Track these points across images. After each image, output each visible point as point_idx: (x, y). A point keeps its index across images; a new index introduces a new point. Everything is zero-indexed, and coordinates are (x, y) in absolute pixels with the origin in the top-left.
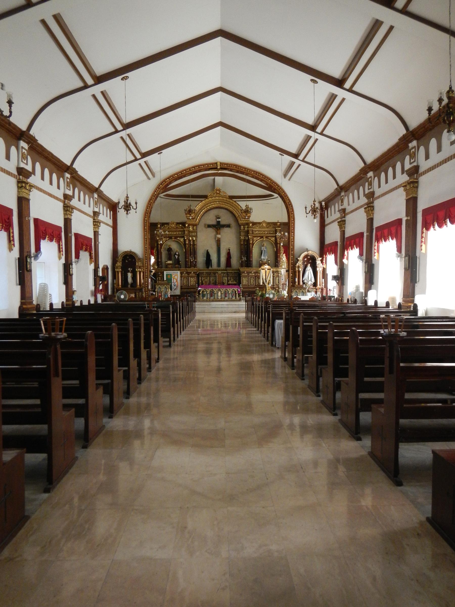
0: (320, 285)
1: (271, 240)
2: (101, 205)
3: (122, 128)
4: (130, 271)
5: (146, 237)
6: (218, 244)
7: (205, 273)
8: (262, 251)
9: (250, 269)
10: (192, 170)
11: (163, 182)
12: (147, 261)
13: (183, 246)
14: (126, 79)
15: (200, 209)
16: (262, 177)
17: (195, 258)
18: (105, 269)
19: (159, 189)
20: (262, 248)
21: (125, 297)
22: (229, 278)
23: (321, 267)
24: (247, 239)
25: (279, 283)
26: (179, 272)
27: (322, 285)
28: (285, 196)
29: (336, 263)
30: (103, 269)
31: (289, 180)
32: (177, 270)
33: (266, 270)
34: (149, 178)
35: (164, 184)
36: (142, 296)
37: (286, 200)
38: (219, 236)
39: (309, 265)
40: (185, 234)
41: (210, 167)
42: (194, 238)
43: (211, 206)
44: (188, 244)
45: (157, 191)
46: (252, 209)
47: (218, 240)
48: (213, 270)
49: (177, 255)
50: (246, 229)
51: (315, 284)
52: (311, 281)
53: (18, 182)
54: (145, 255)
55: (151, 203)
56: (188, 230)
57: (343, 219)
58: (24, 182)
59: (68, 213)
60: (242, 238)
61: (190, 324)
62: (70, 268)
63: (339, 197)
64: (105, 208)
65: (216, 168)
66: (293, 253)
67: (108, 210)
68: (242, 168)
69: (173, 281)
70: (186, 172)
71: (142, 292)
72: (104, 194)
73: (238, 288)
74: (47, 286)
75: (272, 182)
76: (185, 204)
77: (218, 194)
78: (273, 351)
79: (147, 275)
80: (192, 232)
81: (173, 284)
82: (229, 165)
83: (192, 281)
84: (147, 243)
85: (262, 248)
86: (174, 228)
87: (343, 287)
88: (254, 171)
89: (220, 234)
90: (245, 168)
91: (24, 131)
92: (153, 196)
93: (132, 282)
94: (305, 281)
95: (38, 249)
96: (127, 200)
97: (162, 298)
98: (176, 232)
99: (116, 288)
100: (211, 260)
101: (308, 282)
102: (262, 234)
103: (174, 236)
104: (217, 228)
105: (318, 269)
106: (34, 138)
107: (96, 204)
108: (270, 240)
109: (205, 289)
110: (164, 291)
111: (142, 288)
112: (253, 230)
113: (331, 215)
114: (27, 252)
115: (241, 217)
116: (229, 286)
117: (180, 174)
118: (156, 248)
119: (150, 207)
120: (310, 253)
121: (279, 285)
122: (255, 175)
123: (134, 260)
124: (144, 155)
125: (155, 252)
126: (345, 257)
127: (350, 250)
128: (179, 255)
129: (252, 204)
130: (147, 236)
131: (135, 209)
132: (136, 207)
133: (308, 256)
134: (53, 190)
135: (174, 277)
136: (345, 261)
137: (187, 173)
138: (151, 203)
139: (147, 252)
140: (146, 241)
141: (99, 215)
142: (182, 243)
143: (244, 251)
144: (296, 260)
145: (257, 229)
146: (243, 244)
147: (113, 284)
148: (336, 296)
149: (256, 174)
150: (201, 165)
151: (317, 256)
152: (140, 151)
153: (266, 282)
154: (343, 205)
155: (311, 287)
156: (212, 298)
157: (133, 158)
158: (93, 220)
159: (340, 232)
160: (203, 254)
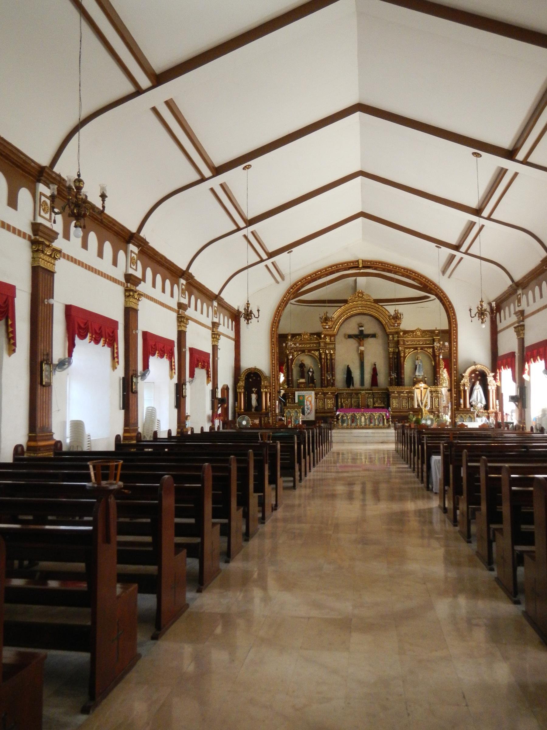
0: (493, 408)
1: (428, 352)
2: (222, 315)
3: (244, 225)
4: (255, 392)
5: (273, 351)
8: (416, 366)
9: (402, 388)
10: (329, 270)
11: (293, 286)
12: (275, 380)
13: (318, 361)
14: (248, 168)
15: (339, 316)
16: (415, 275)
17: (333, 375)
18: (225, 389)
19: (289, 293)
20: (417, 362)
21: (248, 423)
22: (375, 399)
23: (494, 385)
24: (397, 351)
25: (438, 405)
26: (313, 392)
27: (496, 408)
28: (444, 298)
29: (514, 379)
30: (223, 390)
31: (449, 277)
32: (311, 390)
33: (422, 389)
34: (277, 282)
35: (295, 288)
36: (269, 421)
37: (446, 303)
38: (362, 348)
39: (478, 382)
40: (320, 347)
41: (351, 266)
42: (332, 351)
43: (352, 313)
44: (324, 359)
45: (286, 296)
46: (402, 315)
47: (360, 353)
48: (356, 390)
49: (310, 371)
50: (396, 339)
51: (486, 407)
52: (481, 403)
53: (126, 290)
54: (273, 372)
55: (280, 310)
56: (325, 342)
57: (522, 323)
58: (132, 290)
59: (182, 324)
60: (391, 350)
61: (324, 458)
62: (183, 389)
63: (514, 297)
64: (226, 317)
65: (357, 267)
66: (456, 367)
67: (230, 320)
68: (389, 266)
69: (305, 404)
70: (321, 273)
71: (268, 417)
72: (225, 302)
73: (386, 412)
74: (155, 410)
75: (427, 281)
76: (321, 311)
77: (361, 297)
78: (429, 498)
79: (275, 397)
80: (329, 344)
81: (306, 407)
82: (374, 262)
83: (330, 403)
84: (274, 358)
85: (417, 362)
86: (307, 339)
87: (525, 411)
88: (404, 269)
89: (363, 346)
90: (393, 266)
91: (134, 234)
92: (282, 302)
93: (257, 405)
94: (473, 403)
95: (146, 366)
96: (248, 307)
97: (291, 425)
99: (238, 412)
100: (353, 378)
101: (477, 404)
102: (416, 344)
103: (307, 350)
104: (359, 339)
105: (489, 388)
106: (145, 240)
107: (215, 313)
108: (426, 352)
109: (345, 414)
110: (295, 416)
111: (269, 412)
112: (404, 340)
113: (505, 319)
114: (133, 370)
115: (389, 325)
116: (374, 409)
117: (314, 275)
118: (286, 364)
119: (278, 315)
120: (479, 367)
121: (439, 408)
122: (406, 273)
123: (259, 379)
124: (271, 255)
125: (285, 369)
126: (526, 372)
127: (531, 362)
128: (313, 372)
129: (402, 308)
130: (275, 350)
131: (256, 318)
132: (259, 315)
133: (477, 371)
134: (166, 298)
135: (308, 398)
136: (525, 376)
137: (324, 273)
138: (280, 310)
139: (274, 369)
140: (274, 356)
141: (218, 327)
142: (317, 357)
143: (393, 366)
144: (461, 377)
145: (409, 339)
146: (392, 357)
147: (234, 407)
148: (515, 422)
149: (407, 272)
150: (339, 264)
151: (488, 371)
152: (267, 251)
153: (422, 404)
154: (520, 305)
155: (481, 410)
156: (354, 424)
157: (258, 259)
158: (212, 332)
159: (517, 340)
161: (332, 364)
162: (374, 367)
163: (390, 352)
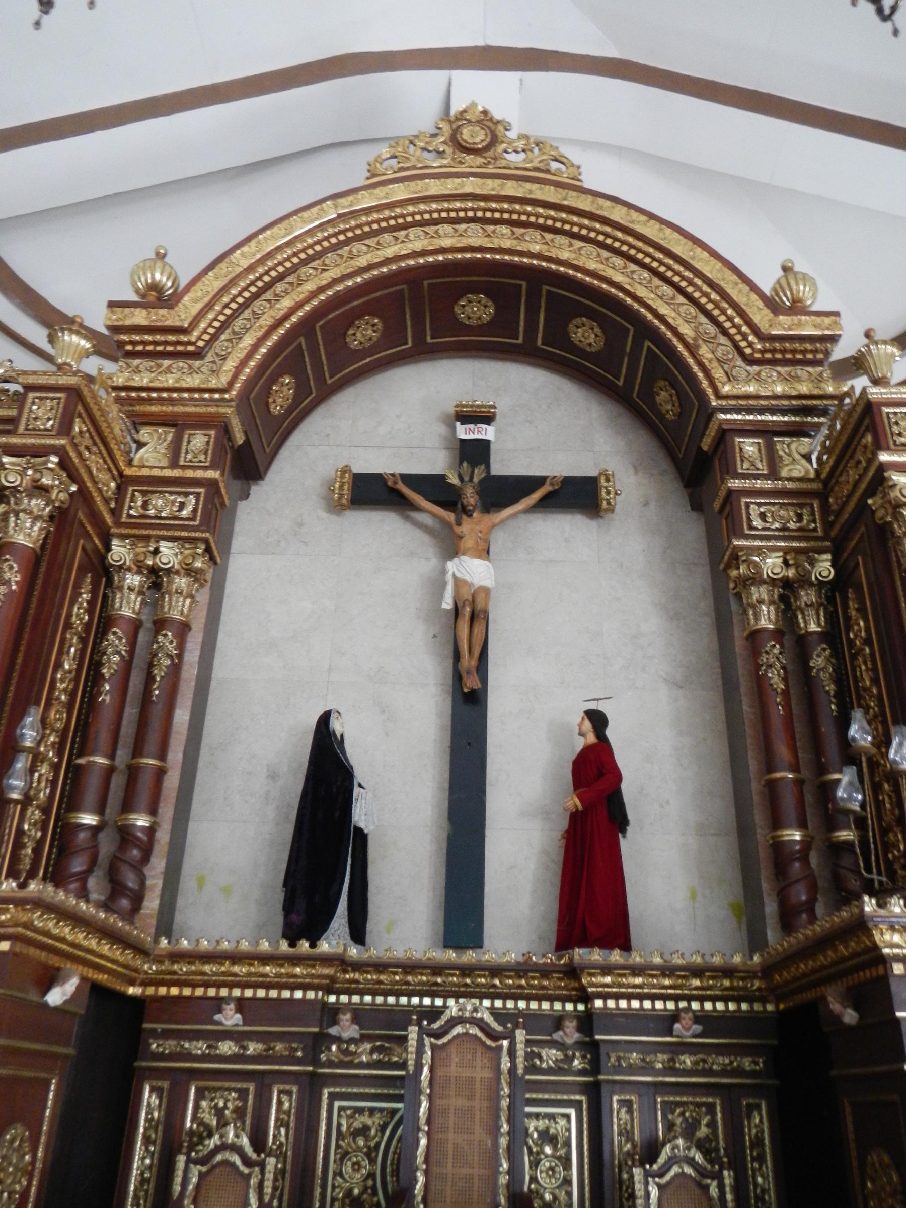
6: (457, 656)
7: (230, 1018)
47: (456, 611)
89: (485, 552)
100: (361, 837)
146: (778, 634)
160: (273, 776)
161: (150, 679)
162: (592, 739)
163: (756, 579)
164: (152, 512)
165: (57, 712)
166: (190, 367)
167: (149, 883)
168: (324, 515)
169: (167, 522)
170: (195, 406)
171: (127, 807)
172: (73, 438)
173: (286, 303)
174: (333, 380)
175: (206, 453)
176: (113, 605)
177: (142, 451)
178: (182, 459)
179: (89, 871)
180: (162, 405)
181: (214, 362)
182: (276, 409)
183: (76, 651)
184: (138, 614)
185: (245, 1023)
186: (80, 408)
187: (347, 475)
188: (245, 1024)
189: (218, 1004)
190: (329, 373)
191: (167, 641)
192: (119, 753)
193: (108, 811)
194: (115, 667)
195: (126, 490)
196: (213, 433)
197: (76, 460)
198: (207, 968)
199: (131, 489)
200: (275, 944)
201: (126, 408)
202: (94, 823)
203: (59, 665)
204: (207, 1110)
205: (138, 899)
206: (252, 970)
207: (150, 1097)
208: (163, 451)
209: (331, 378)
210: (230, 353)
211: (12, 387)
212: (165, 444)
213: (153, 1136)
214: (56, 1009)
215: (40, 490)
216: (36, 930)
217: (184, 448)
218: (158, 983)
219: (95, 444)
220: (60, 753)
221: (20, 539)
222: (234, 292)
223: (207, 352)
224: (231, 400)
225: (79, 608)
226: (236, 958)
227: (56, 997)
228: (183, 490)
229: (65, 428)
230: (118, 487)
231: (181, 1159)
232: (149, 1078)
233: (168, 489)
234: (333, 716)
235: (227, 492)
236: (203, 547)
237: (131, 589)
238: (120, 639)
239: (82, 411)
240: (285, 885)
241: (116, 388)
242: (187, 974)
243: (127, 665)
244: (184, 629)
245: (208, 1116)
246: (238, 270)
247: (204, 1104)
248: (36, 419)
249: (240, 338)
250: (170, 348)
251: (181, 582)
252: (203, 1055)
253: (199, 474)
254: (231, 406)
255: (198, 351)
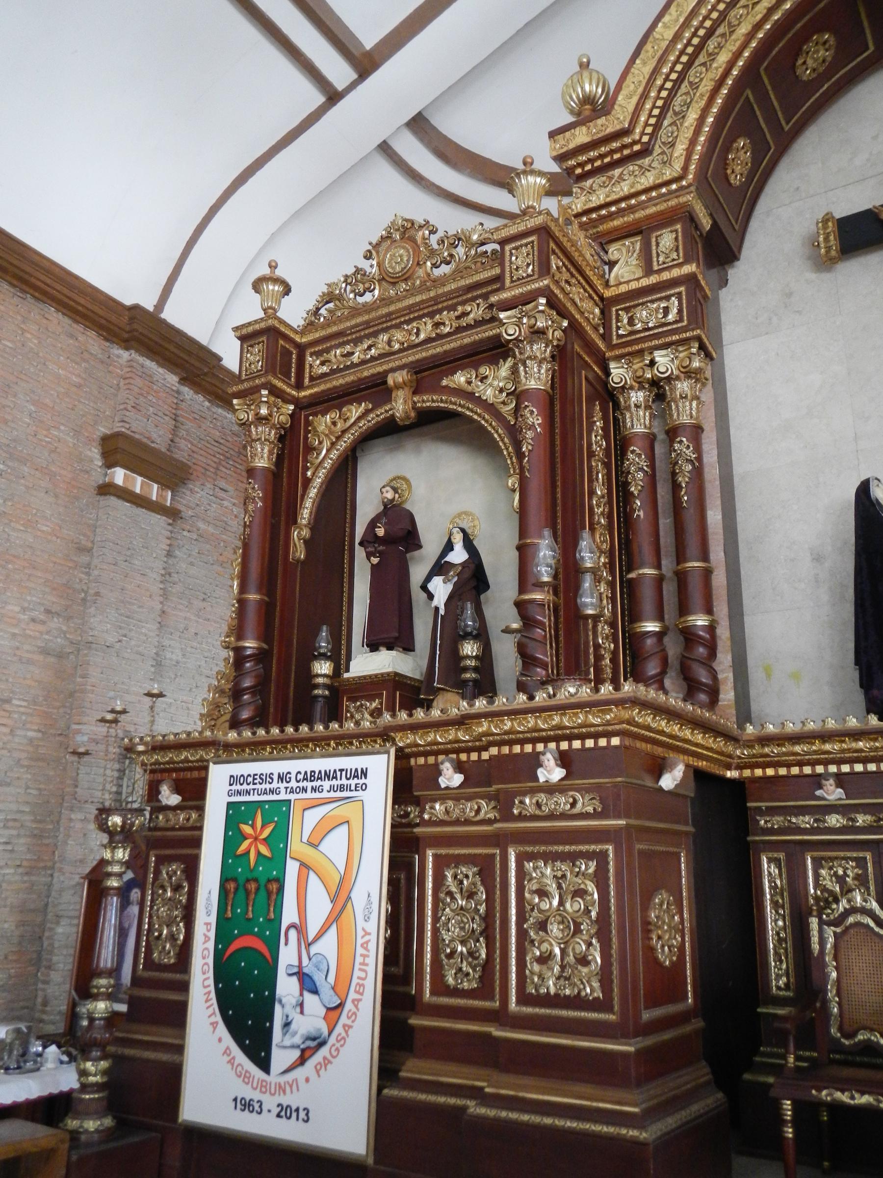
7: (832, 793)
69: (290, 915)
81: (288, 955)
98: (431, 315)
160: (818, 558)
161: (676, 487)
164: (639, 326)
165: (601, 535)
166: (640, 167)
167: (720, 676)
168: (812, 276)
169: (656, 331)
170: (655, 205)
171: (684, 609)
172: (553, 276)
173: (723, 58)
174: (791, 124)
175: (677, 250)
176: (625, 426)
177: (616, 269)
178: (655, 263)
179: (663, 673)
180: (623, 216)
181: (663, 153)
182: (736, 180)
183: (603, 476)
184: (650, 428)
185: (848, 797)
186: (552, 245)
187: (830, 224)
188: (848, 798)
189: (817, 781)
190: (785, 119)
191: (684, 446)
192: (664, 562)
193: (666, 617)
194: (641, 483)
195: (610, 312)
196: (678, 227)
197: (561, 296)
198: (798, 749)
199: (614, 309)
200: (863, 720)
201: (591, 232)
202: (657, 629)
203: (592, 493)
204: (828, 878)
205: (714, 693)
206: (844, 746)
207: (769, 867)
208: (635, 262)
209: (787, 123)
210: (677, 137)
211: (489, 248)
212: (635, 255)
213: (780, 901)
214: (669, 792)
215: (538, 333)
216: (638, 725)
217: (654, 252)
218: (753, 766)
219: (573, 276)
220: (612, 572)
221: (532, 384)
222: (665, 70)
223: (654, 144)
224: (689, 185)
225: (596, 436)
226: (825, 736)
227: (668, 782)
228: (663, 294)
229: (544, 269)
230: (602, 312)
231: (814, 922)
232: (764, 851)
233: (650, 298)
234: (873, 485)
235: (707, 283)
236: (697, 345)
237: (637, 406)
238: (639, 456)
239: (554, 247)
240: (858, 661)
241: (578, 215)
242: (778, 755)
243: (652, 478)
244: (697, 430)
245: (829, 883)
246: (664, 44)
247: (823, 872)
248: (517, 269)
249: (684, 117)
250: (617, 156)
251: (683, 386)
252: (812, 828)
253: (676, 273)
254: (691, 192)
255: (645, 146)
